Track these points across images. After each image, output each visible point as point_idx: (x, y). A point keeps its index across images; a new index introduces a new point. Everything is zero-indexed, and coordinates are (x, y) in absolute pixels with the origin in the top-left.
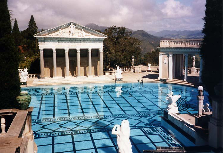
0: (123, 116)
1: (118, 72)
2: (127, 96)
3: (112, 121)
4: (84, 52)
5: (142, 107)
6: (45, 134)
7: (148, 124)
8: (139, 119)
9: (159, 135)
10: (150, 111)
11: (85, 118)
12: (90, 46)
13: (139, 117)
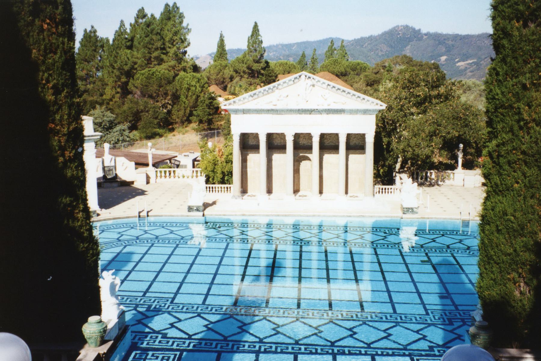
0: (387, 318)
2: (417, 260)
3: (355, 330)
6: (206, 344)
7: (439, 346)
8: (421, 330)
10: (457, 309)
11: (298, 313)
13: (423, 326)
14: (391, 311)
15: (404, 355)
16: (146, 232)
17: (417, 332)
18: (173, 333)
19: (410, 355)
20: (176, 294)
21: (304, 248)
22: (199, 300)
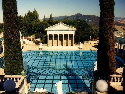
1: (81, 45)
2: (83, 58)
4: (66, 36)
5: (87, 65)
7: (87, 74)
9: (89, 80)
12: (69, 33)
14: (78, 68)
15: (81, 76)
16: (31, 53)
17: (83, 72)
18: (37, 73)
19: (82, 76)
20: (38, 65)
21: (62, 56)
22: (42, 66)
